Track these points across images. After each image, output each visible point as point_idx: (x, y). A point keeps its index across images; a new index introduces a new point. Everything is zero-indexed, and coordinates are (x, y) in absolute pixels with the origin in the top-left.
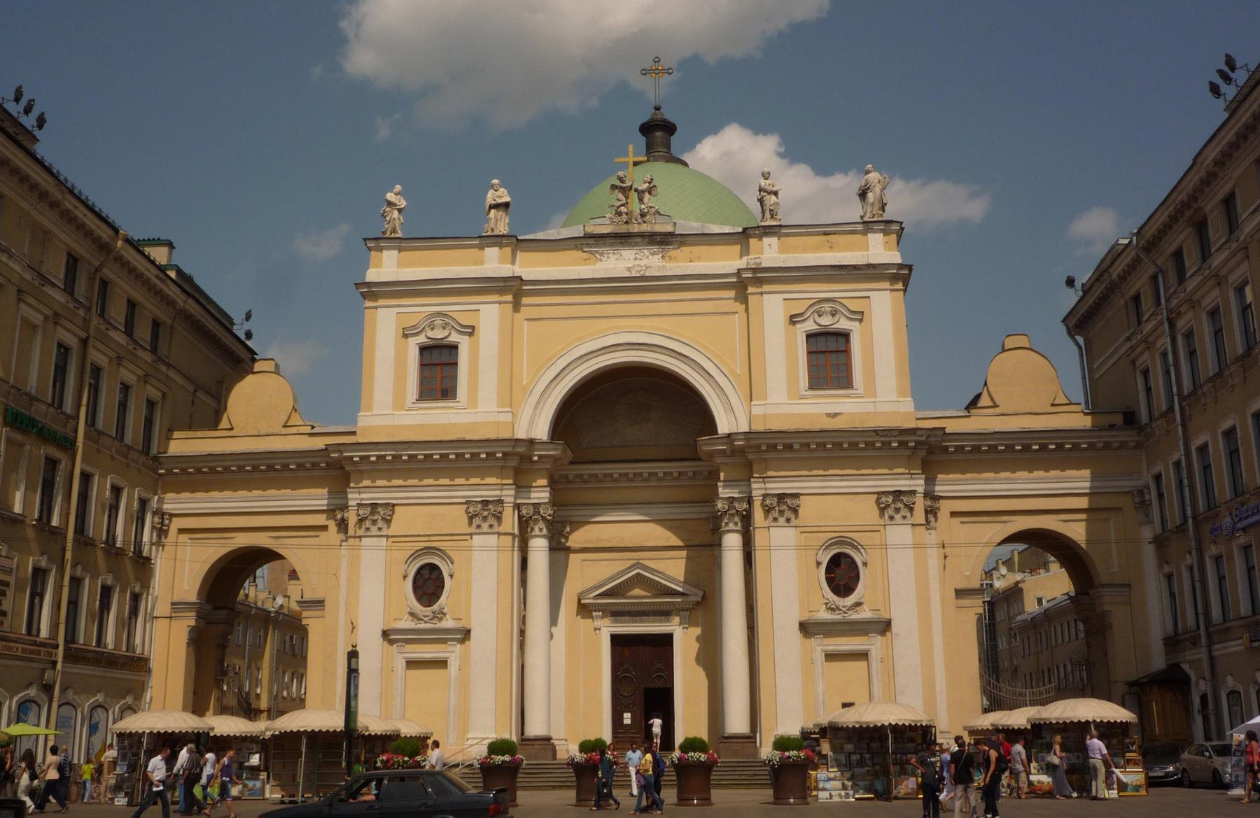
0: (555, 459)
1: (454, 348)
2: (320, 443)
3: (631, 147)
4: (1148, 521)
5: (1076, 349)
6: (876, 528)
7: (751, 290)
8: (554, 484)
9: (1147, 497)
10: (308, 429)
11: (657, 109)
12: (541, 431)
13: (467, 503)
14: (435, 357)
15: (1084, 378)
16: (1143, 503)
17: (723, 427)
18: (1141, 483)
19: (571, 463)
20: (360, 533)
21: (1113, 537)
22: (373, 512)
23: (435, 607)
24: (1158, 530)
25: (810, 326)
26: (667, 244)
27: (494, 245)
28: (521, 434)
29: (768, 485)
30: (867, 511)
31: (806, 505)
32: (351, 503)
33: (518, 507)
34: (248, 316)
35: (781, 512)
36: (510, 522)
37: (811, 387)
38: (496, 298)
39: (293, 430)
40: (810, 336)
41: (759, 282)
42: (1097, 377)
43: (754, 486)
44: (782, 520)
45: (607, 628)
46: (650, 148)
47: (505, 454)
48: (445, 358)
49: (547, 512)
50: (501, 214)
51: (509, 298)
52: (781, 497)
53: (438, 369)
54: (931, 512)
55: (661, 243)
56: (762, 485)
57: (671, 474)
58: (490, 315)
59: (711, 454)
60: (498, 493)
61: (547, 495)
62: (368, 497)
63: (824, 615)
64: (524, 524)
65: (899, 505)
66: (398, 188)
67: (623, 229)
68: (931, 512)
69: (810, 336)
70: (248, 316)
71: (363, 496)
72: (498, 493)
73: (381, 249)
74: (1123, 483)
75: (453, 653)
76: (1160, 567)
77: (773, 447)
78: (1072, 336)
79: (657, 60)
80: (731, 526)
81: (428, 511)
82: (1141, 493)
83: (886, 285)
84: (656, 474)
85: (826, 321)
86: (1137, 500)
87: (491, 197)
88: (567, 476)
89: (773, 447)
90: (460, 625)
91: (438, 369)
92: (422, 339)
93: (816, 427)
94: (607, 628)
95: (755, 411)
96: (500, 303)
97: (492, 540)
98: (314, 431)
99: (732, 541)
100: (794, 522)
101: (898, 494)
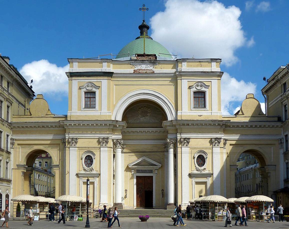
0: (123, 126)
2: (57, 120)
4: (282, 147)
5: (264, 98)
6: (210, 148)
9: (283, 141)
10: (53, 116)
11: (144, 21)
12: (119, 118)
13: (99, 138)
15: (266, 107)
16: (281, 143)
17: (170, 118)
18: (281, 137)
19: (127, 128)
20: (68, 146)
21: (272, 152)
22: (72, 140)
24: (285, 150)
28: (113, 119)
29: (182, 135)
30: (208, 145)
32: (66, 138)
33: (113, 140)
34: (32, 81)
36: (111, 144)
39: (49, 116)
42: (270, 107)
43: (178, 135)
46: (142, 33)
47: (109, 125)
52: (185, 139)
54: (225, 144)
56: (180, 135)
57: (153, 131)
59: (166, 126)
60: (107, 136)
61: (121, 137)
62: (71, 136)
64: (114, 144)
65: (216, 142)
68: (225, 144)
70: (32, 81)
71: (70, 135)
72: (107, 136)
74: (276, 137)
76: (285, 161)
77: (184, 125)
78: (263, 95)
79: (144, 5)
80: (171, 147)
81: (87, 141)
82: (281, 140)
84: (149, 131)
86: (280, 142)
89: (184, 125)
93: (195, 119)
97: (106, 149)
98: (55, 116)
99: (171, 151)
100: (189, 146)
101: (216, 139)
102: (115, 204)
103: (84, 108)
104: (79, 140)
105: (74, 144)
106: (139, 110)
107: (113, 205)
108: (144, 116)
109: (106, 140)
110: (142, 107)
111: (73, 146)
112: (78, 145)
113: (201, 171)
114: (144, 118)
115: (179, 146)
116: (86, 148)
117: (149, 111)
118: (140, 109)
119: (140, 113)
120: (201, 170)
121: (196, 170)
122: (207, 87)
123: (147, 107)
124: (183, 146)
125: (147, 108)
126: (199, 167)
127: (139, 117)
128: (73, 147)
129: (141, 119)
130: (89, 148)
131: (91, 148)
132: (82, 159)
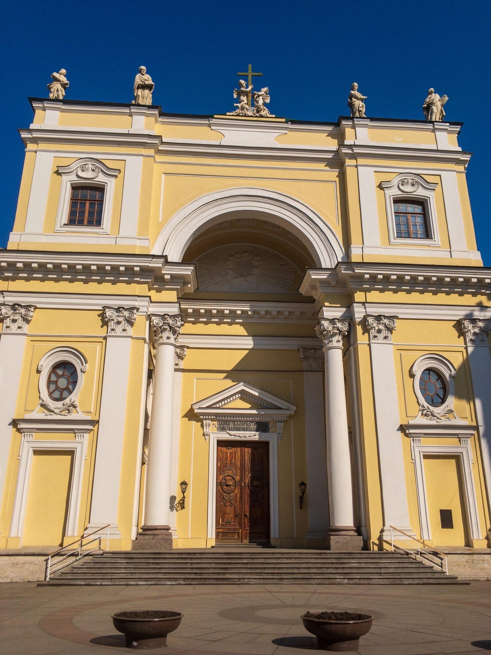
3: (250, 66)
23: (67, 401)
33: (149, 317)
36: (142, 328)
37: (400, 235)
41: (354, 156)
44: (381, 336)
45: (215, 434)
53: (87, 204)
58: (134, 164)
63: (422, 420)
64: (155, 333)
75: (82, 444)
80: (335, 344)
85: (408, 188)
90: (89, 418)
91: (87, 204)
92: (73, 177)
94: (215, 434)
102: (147, 531)
103: (65, 224)
104: (34, 315)
105: (20, 322)
107: (139, 534)
108: (242, 276)
109: (128, 315)
110: (237, 253)
111: (14, 331)
113: (438, 418)
115: (361, 338)
120: (439, 416)
121: (422, 415)
122: (429, 186)
124: (373, 341)
126: (430, 407)
132: (39, 372)
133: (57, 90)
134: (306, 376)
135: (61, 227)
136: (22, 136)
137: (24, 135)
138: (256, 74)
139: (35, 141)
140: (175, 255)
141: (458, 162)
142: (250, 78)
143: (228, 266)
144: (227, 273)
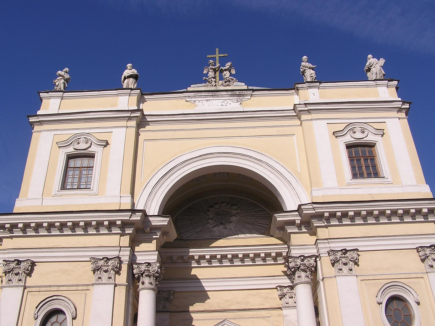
1: (92, 156)
3: (217, 49)
6: (420, 276)
7: (304, 117)
8: (162, 248)
14: (78, 162)
25: (348, 139)
26: (243, 95)
27: (125, 94)
29: (332, 245)
31: (363, 259)
35: (345, 264)
38: (124, 123)
40: (349, 147)
48: (85, 162)
49: (155, 267)
50: (131, 80)
51: (133, 123)
55: (239, 95)
56: (328, 245)
60: (116, 253)
61: (156, 257)
66: (67, 69)
67: (213, 88)
69: (349, 147)
73: (49, 98)
83: (394, 114)
85: (358, 135)
87: (127, 73)
88: (171, 257)
92: (70, 150)
95: (315, 193)
96: (127, 127)
106: (208, 211)
108: (222, 224)
111: (14, 284)
112: (30, 281)
114: (221, 227)
116: (52, 289)
117: (234, 212)
118: (211, 207)
119: (211, 216)
123: (228, 204)
125: (229, 206)
127: (208, 225)
128: (13, 287)
129: (215, 229)
130: (61, 288)
131: (65, 288)
133: (60, 83)
134: (285, 312)
135: (58, 191)
136: (30, 121)
137: (32, 120)
138: (222, 55)
139: (41, 123)
140: (154, 209)
141: (400, 110)
142: (217, 58)
143: (209, 216)
144: (208, 223)
